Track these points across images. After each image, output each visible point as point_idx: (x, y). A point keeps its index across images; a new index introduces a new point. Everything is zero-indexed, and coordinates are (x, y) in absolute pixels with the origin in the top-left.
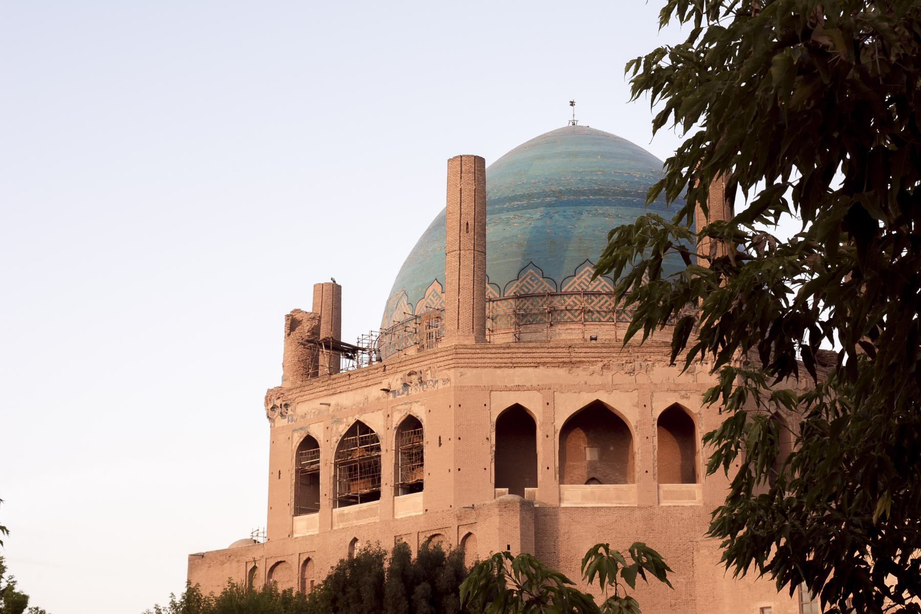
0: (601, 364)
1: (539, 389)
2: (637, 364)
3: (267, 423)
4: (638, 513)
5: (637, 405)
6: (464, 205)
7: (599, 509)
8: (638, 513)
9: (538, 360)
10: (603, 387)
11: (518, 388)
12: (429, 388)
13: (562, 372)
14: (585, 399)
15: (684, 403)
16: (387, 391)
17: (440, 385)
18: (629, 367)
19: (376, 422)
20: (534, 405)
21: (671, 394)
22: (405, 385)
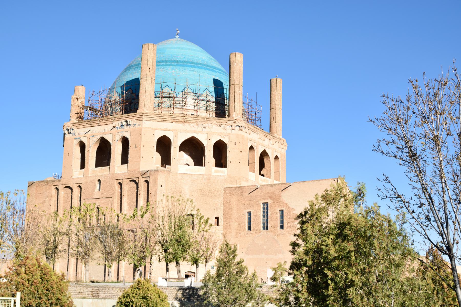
2: (207, 125)
4: (205, 177)
10: (195, 132)
11: (166, 130)
12: (131, 127)
13: (181, 125)
16: (114, 127)
17: (136, 126)
19: (109, 138)
20: (170, 135)
22: (122, 126)
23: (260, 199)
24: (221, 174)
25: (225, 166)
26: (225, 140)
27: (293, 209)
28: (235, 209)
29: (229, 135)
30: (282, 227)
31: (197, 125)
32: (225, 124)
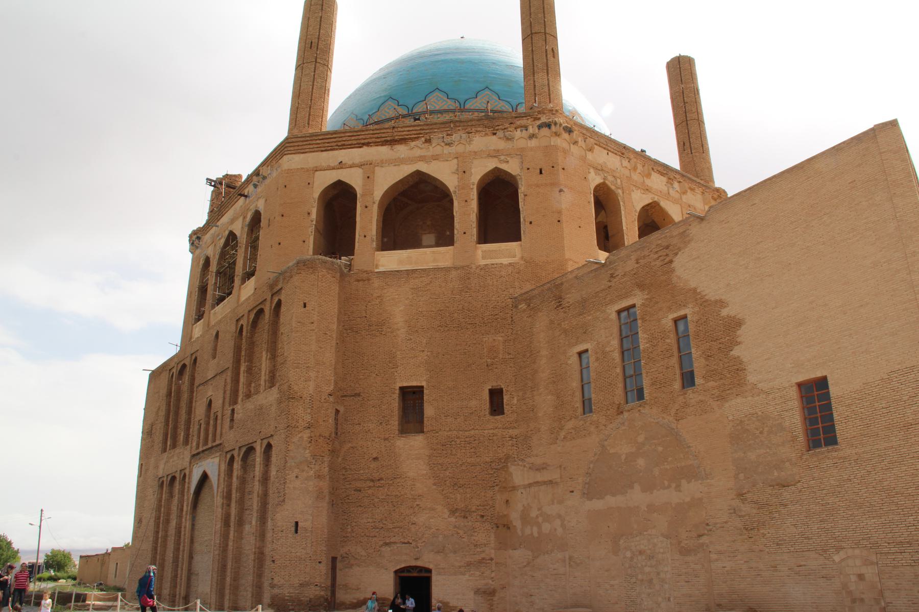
0: (423, 139)
1: (361, 166)
2: (455, 137)
3: (191, 255)
4: (454, 274)
5: (456, 172)
6: (310, 29)
7: (414, 271)
8: (454, 274)
9: (363, 141)
10: (422, 159)
11: (341, 165)
13: (384, 151)
14: (407, 170)
15: (504, 167)
18: (448, 139)
20: (354, 178)
21: (491, 160)
23: (612, 302)
24: (505, 261)
25: (517, 237)
26: (512, 167)
27: (721, 304)
28: (544, 352)
29: (521, 154)
30: (688, 379)
31: (428, 141)
32: (507, 125)
